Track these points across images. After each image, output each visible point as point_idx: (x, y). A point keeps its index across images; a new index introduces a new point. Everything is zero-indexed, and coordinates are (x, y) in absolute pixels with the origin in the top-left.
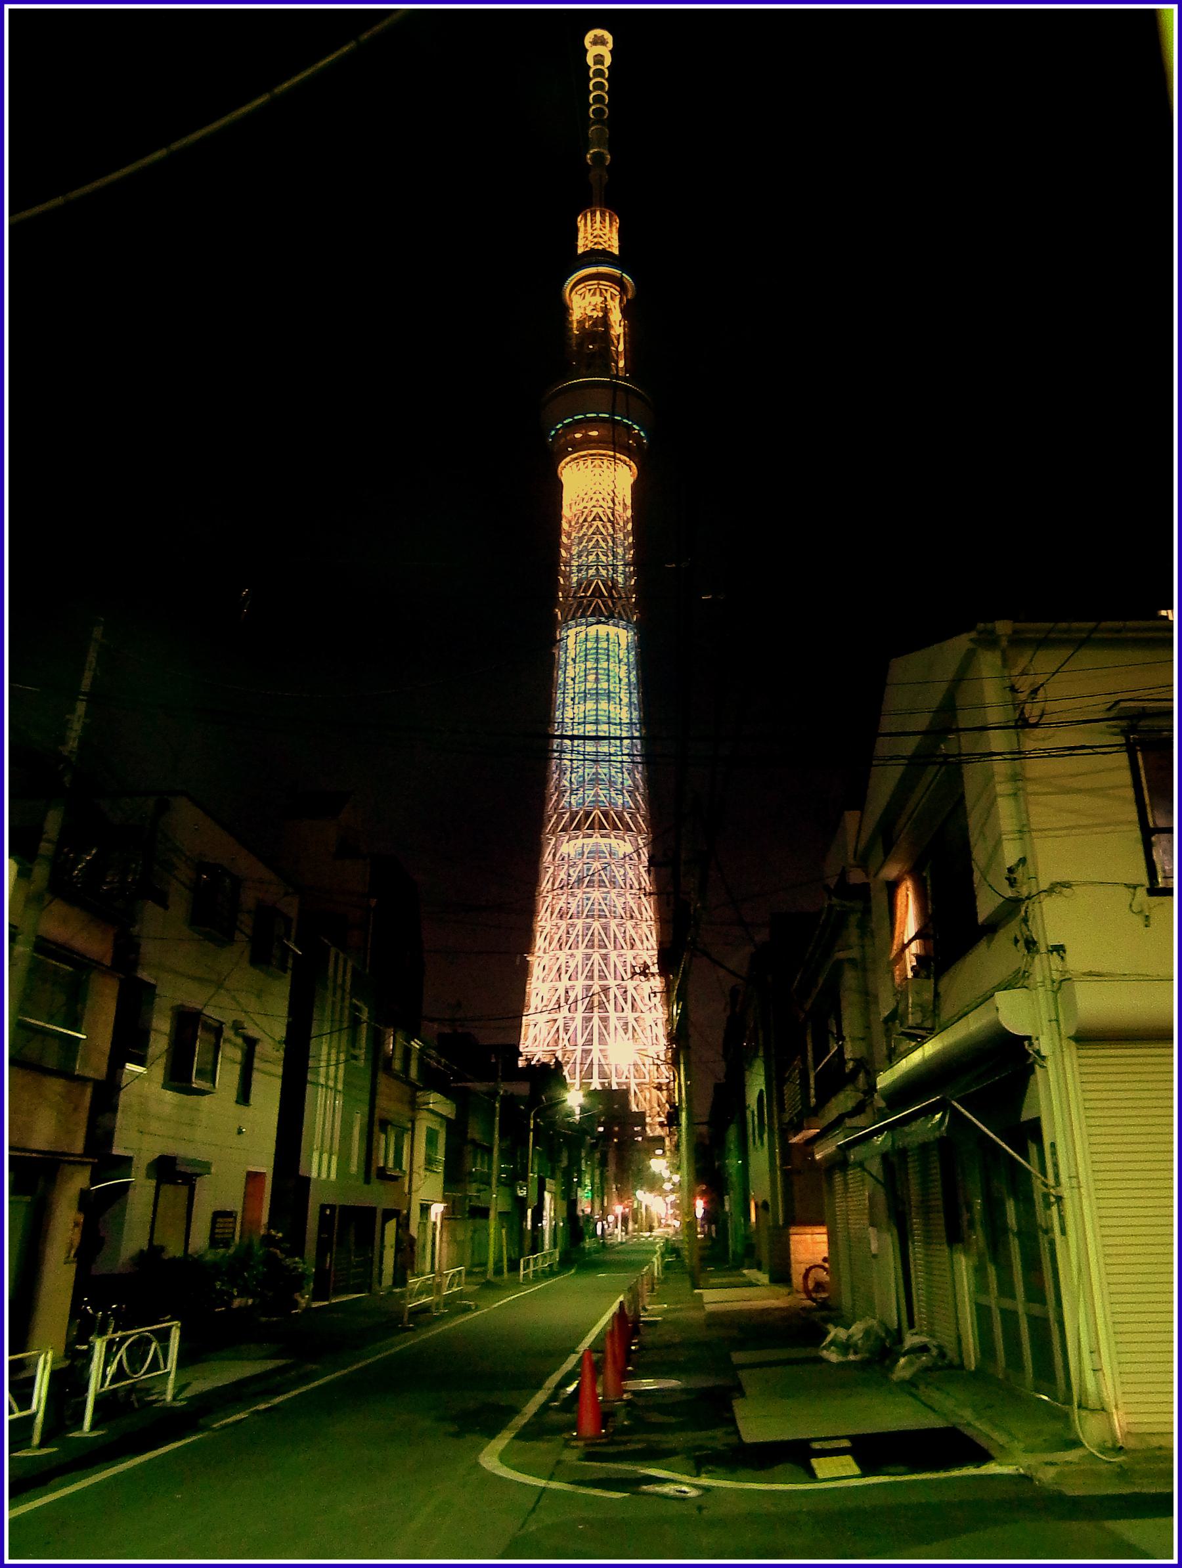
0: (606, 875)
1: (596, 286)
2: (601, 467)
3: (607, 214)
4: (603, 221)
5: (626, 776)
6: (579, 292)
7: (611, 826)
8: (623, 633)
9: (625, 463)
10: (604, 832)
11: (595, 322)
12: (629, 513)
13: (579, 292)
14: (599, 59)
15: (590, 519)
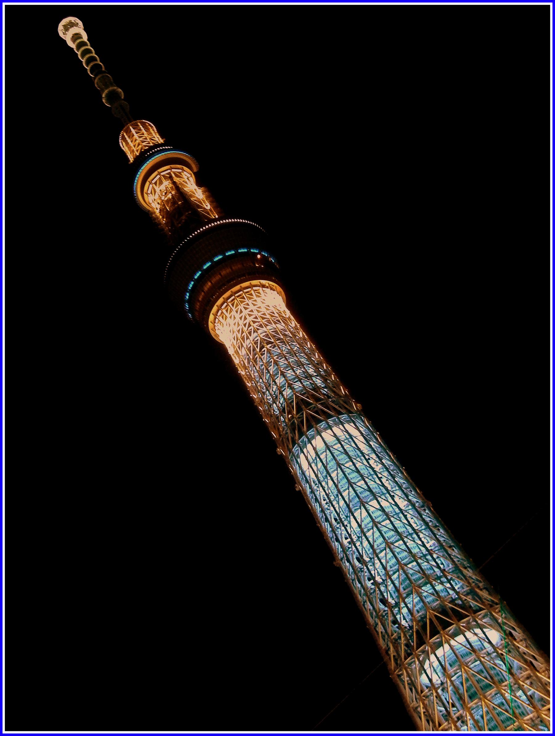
0: (486, 678)
1: (158, 176)
2: (242, 302)
3: (139, 124)
4: (138, 131)
5: (508, 658)
6: (149, 192)
7: (454, 618)
8: (350, 428)
9: (263, 286)
10: (451, 629)
11: (173, 201)
12: (294, 323)
13: (149, 192)
14: (76, 37)
15: (258, 350)
